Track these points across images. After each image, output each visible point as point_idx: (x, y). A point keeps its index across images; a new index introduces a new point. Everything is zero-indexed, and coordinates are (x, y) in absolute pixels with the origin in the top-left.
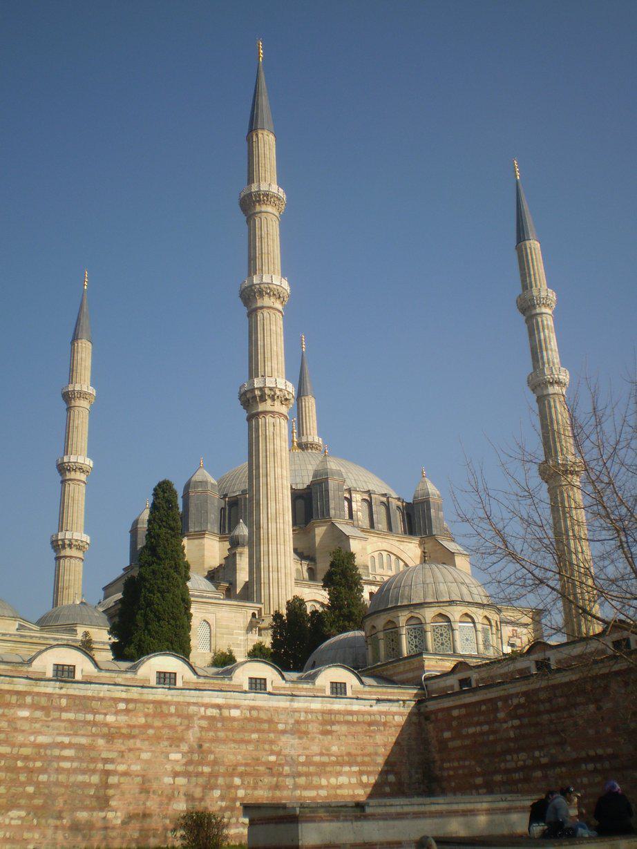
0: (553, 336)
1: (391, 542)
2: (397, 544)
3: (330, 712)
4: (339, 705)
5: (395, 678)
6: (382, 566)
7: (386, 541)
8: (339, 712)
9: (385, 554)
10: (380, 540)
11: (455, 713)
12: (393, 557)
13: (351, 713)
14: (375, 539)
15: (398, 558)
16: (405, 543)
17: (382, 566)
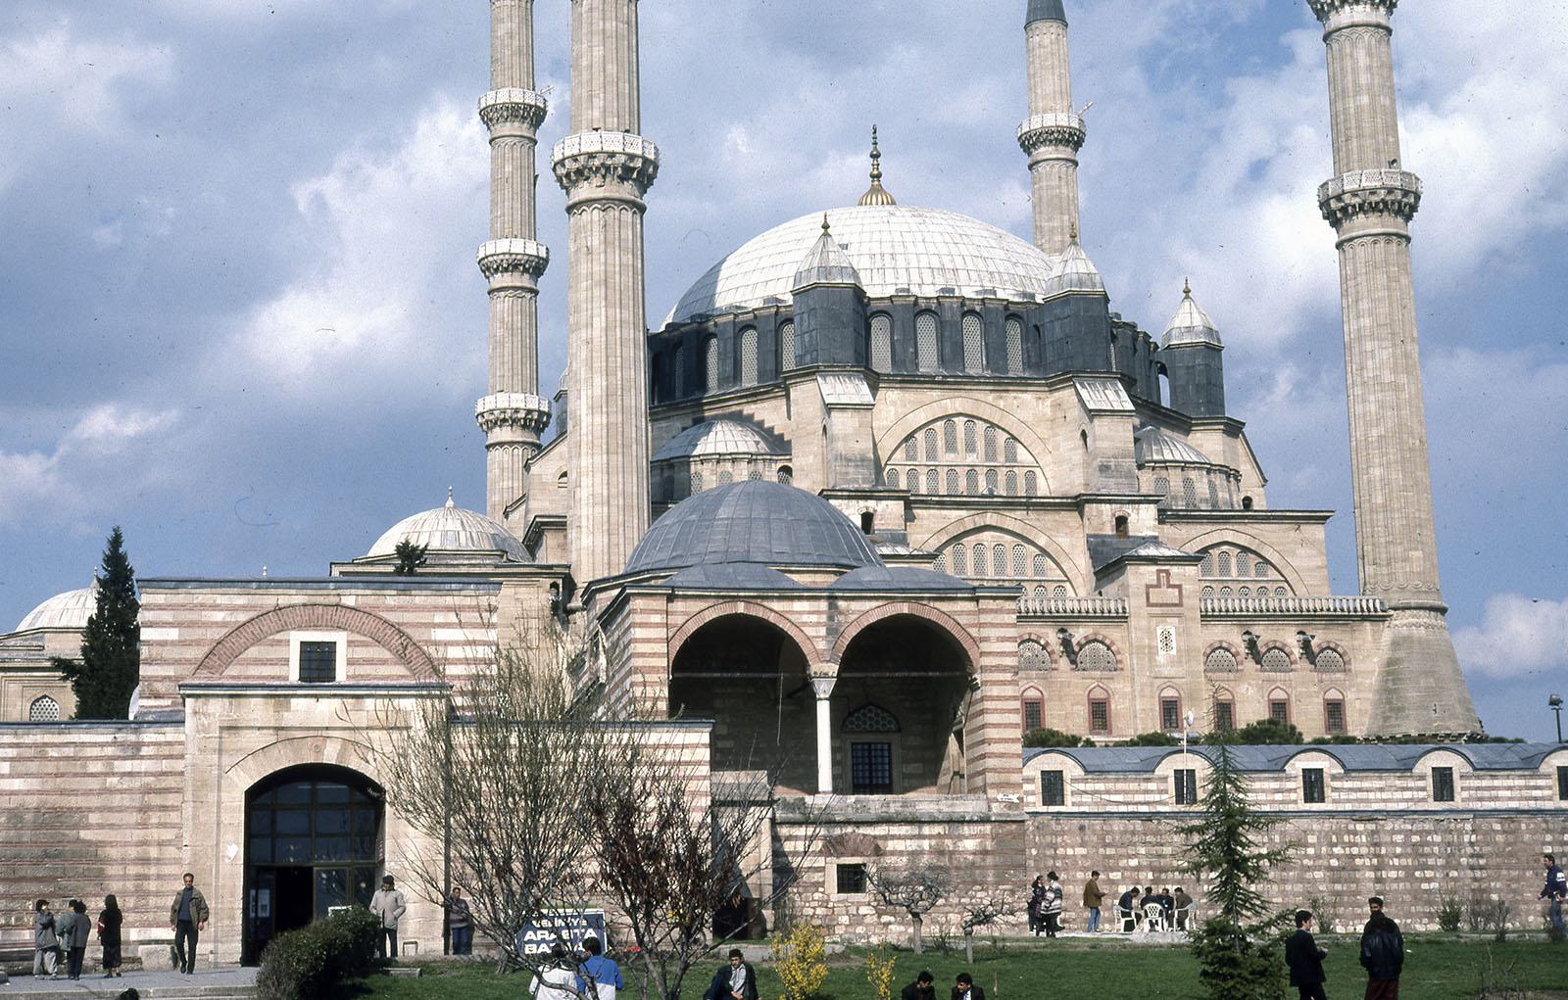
2: (990, 397)
6: (951, 447)
7: (963, 393)
9: (960, 422)
12: (981, 426)
16: (1014, 394)
17: (951, 447)
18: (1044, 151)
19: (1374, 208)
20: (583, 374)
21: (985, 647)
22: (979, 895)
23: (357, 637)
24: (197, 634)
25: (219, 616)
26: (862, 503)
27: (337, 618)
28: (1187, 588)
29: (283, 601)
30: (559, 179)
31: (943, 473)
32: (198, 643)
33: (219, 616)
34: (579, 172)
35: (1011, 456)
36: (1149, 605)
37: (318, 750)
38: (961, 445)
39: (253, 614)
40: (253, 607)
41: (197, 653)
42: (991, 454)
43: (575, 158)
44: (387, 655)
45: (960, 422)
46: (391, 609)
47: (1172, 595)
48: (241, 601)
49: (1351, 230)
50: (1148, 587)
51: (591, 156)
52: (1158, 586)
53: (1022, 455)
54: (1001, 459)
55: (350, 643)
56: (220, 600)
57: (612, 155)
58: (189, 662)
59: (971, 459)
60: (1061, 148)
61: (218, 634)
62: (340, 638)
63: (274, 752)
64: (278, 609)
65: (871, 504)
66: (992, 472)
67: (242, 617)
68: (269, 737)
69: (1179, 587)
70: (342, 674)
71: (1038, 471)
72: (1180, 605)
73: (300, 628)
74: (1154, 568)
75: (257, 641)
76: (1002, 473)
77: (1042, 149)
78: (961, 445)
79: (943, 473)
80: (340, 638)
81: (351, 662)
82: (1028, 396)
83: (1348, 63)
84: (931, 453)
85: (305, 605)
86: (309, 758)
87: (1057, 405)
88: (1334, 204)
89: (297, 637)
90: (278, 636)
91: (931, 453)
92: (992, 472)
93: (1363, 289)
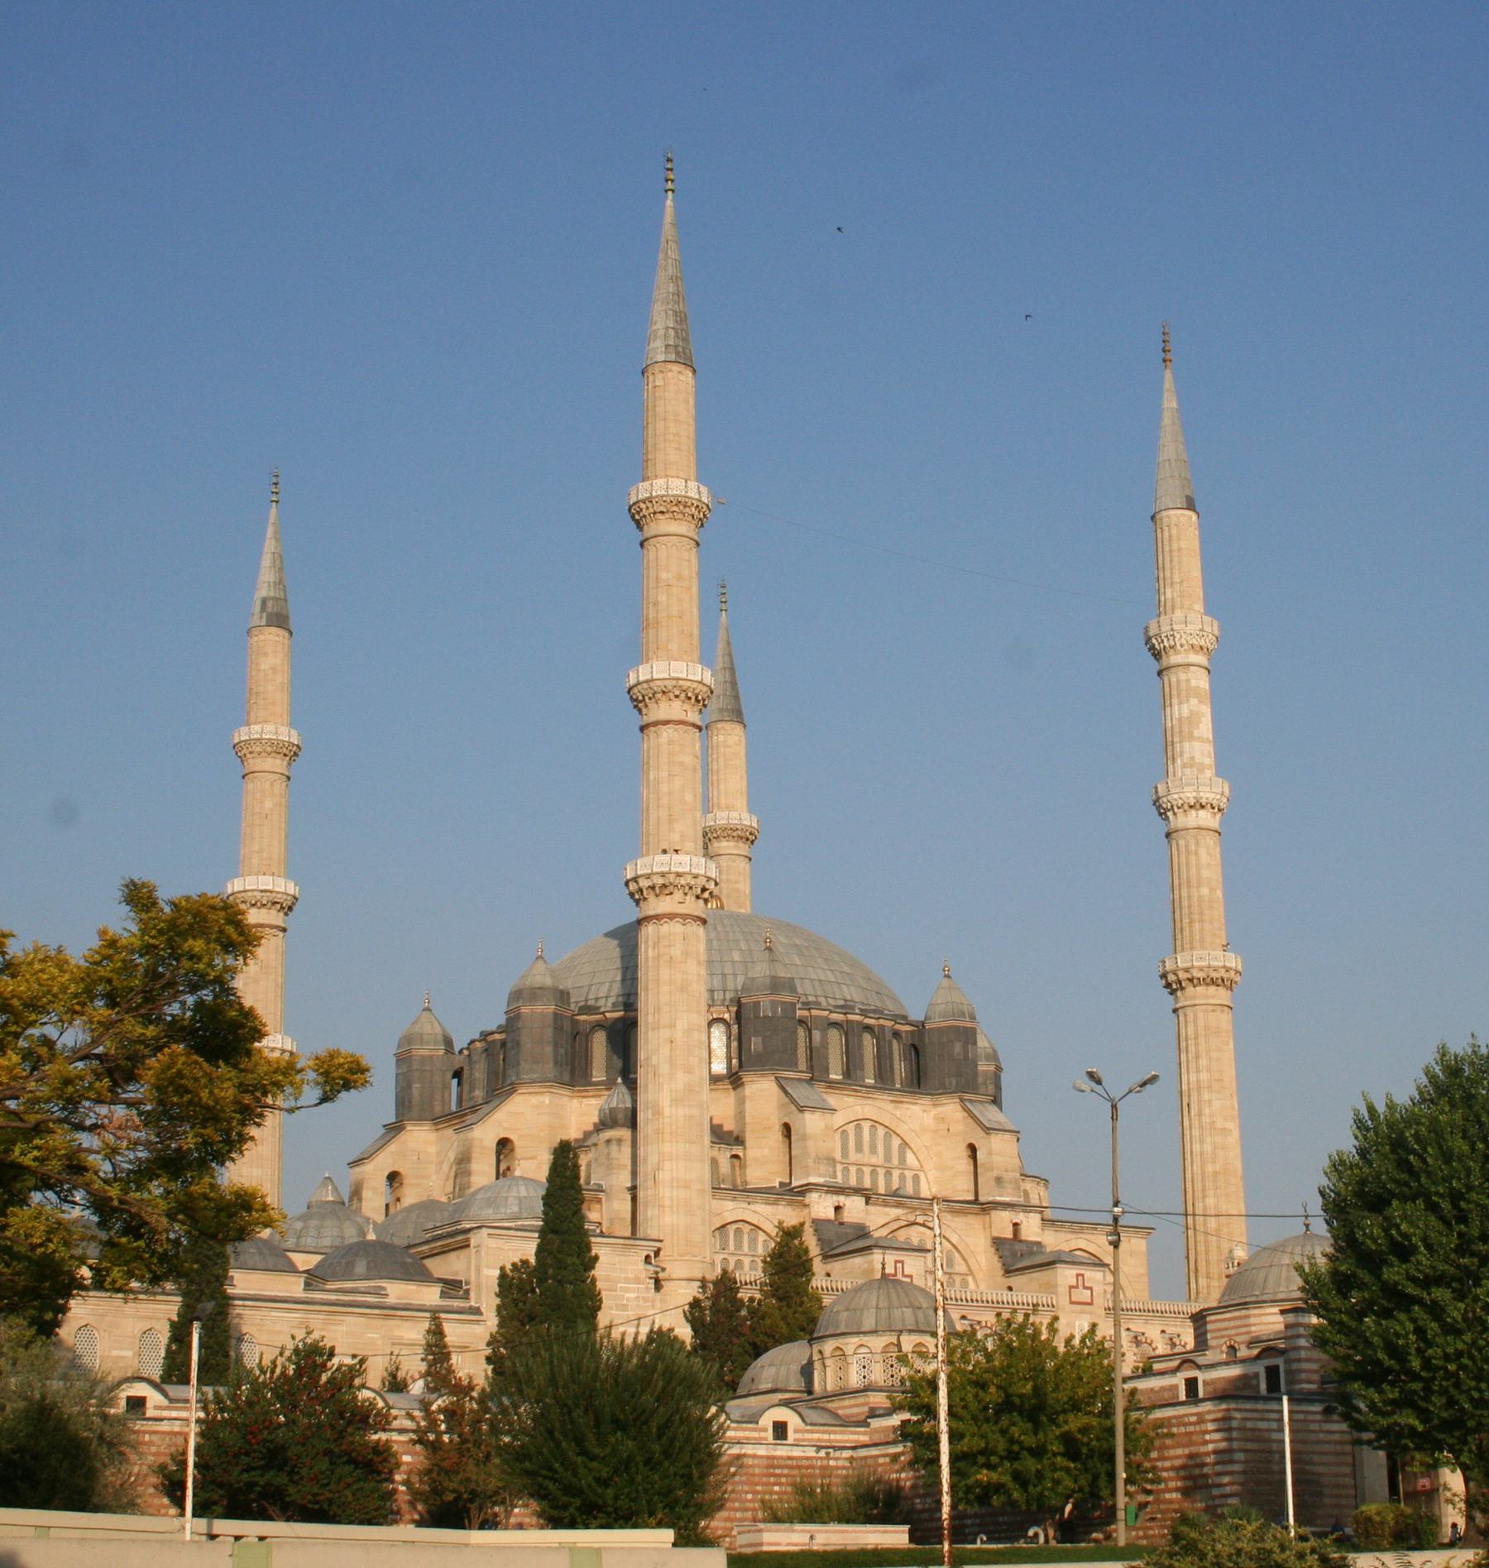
0: (1206, 710)
1: (879, 1103)
2: (890, 1107)
3: (774, 1458)
4: (781, 1451)
5: (840, 1412)
6: (859, 1148)
8: (781, 1458)
9: (866, 1126)
10: (861, 1101)
11: (881, 1460)
12: (881, 1131)
13: (790, 1458)
14: (851, 1099)
15: (890, 1132)
17: (859, 1148)
18: (724, 846)
19: (1213, 982)
20: (665, 1069)
26: (835, 1198)
28: (1097, 1290)
30: (632, 895)
31: (853, 1169)
35: (902, 1159)
36: (1072, 1303)
38: (866, 1148)
42: (888, 1157)
43: (663, 875)
45: (866, 1126)
47: (1085, 1295)
49: (1193, 997)
50: (1071, 1287)
51: (679, 875)
52: (1076, 1287)
53: (911, 1159)
54: (895, 1161)
57: (696, 877)
59: (874, 1160)
60: (741, 845)
65: (842, 1199)
66: (888, 1174)
69: (1091, 1289)
71: (922, 1175)
72: (1091, 1304)
74: (1074, 1272)
76: (896, 1173)
77: (724, 844)
78: (866, 1148)
79: (853, 1169)
82: (916, 1108)
83: (1193, 858)
84: (845, 1154)
87: (941, 1119)
88: (1171, 978)
91: (845, 1154)
92: (888, 1174)
93: (1202, 1047)
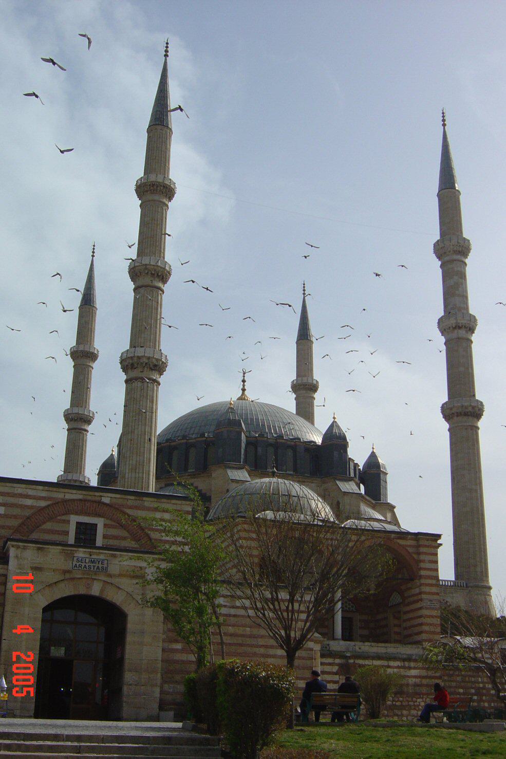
21: (422, 565)
22: (418, 700)
23: (109, 522)
24: (16, 511)
25: (29, 502)
27: (97, 508)
29: (68, 496)
32: (15, 517)
33: (29, 502)
34: (132, 365)
37: (89, 587)
39: (49, 503)
40: (49, 499)
41: (16, 523)
44: (126, 534)
46: (131, 507)
48: (44, 494)
55: (105, 526)
56: (31, 492)
57: (149, 358)
58: (9, 527)
61: (28, 513)
62: (100, 522)
63: (62, 585)
64: (65, 501)
67: (43, 504)
68: (58, 577)
70: (99, 542)
73: (76, 513)
75: (51, 519)
80: (100, 522)
81: (105, 537)
85: (80, 500)
86: (82, 591)
89: (74, 519)
90: (64, 517)
